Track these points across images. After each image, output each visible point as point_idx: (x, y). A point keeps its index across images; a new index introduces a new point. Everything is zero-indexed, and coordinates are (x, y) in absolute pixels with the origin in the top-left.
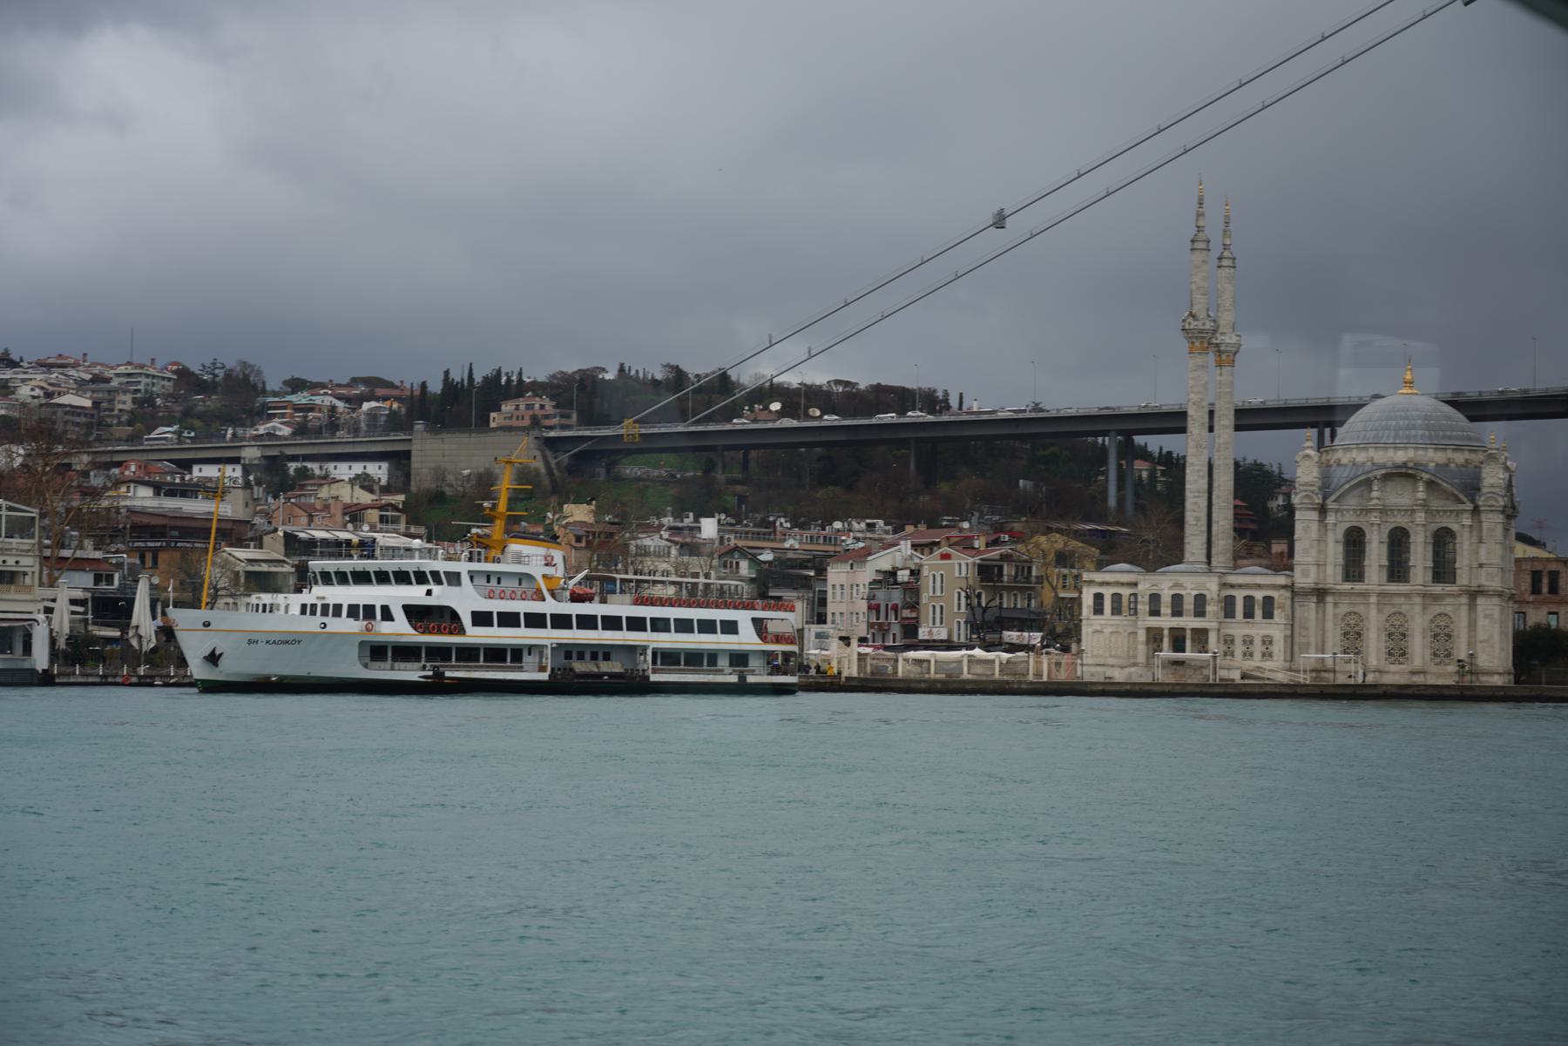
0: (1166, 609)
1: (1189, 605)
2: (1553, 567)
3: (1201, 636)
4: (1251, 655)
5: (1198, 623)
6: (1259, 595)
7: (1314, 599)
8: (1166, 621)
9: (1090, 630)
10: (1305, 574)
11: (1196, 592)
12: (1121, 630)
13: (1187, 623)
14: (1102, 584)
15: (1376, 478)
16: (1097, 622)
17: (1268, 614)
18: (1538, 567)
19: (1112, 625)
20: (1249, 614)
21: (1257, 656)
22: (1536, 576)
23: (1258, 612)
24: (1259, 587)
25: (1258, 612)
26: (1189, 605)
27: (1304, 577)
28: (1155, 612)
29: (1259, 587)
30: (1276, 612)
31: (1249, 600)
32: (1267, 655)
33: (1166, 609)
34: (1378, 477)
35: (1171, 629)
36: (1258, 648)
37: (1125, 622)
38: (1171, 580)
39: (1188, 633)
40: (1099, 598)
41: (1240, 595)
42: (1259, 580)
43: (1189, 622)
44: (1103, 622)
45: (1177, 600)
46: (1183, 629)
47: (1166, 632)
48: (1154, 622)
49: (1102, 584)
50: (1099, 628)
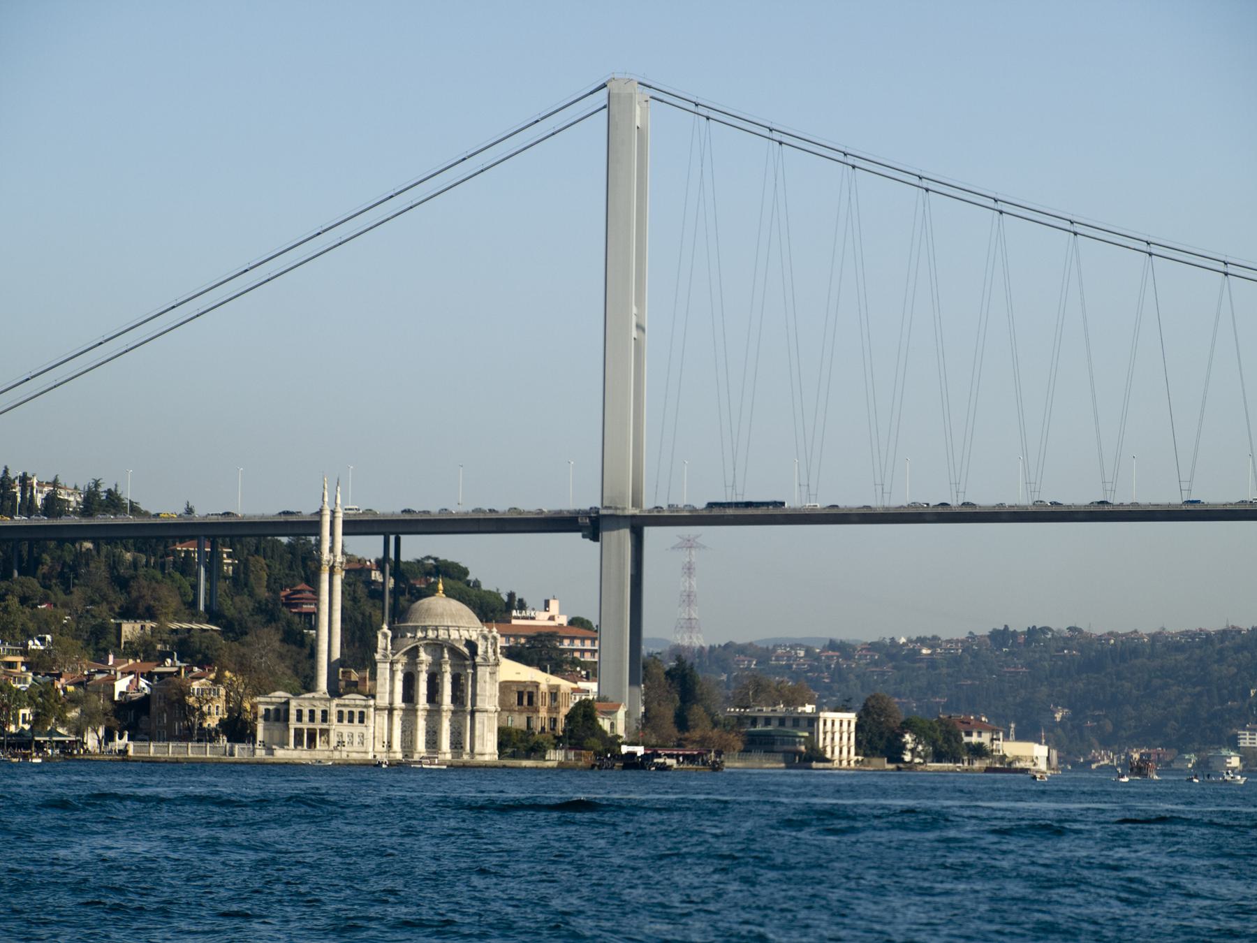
0: (306, 718)
1: (318, 715)
2: (530, 689)
3: (325, 732)
4: (352, 743)
5: (325, 726)
6: (356, 711)
7: (387, 712)
8: (306, 725)
10: (382, 698)
17: (361, 721)
18: (521, 689)
20: (351, 721)
21: (355, 743)
22: (520, 695)
23: (356, 720)
24: (356, 706)
25: (356, 720)
26: (318, 715)
27: (383, 700)
28: (299, 718)
29: (356, 706)
31: (351, 713)
33: (306, 718)
35: (308, 729)
36: (356, 739)
39: (318, 731)
40: (267, 711)
41: (346, 710)
42: (358, 702)
43: (318, 725)
45: (312, 712)
46: (315, 729)
47: (306, 731)
48: (299, 725)
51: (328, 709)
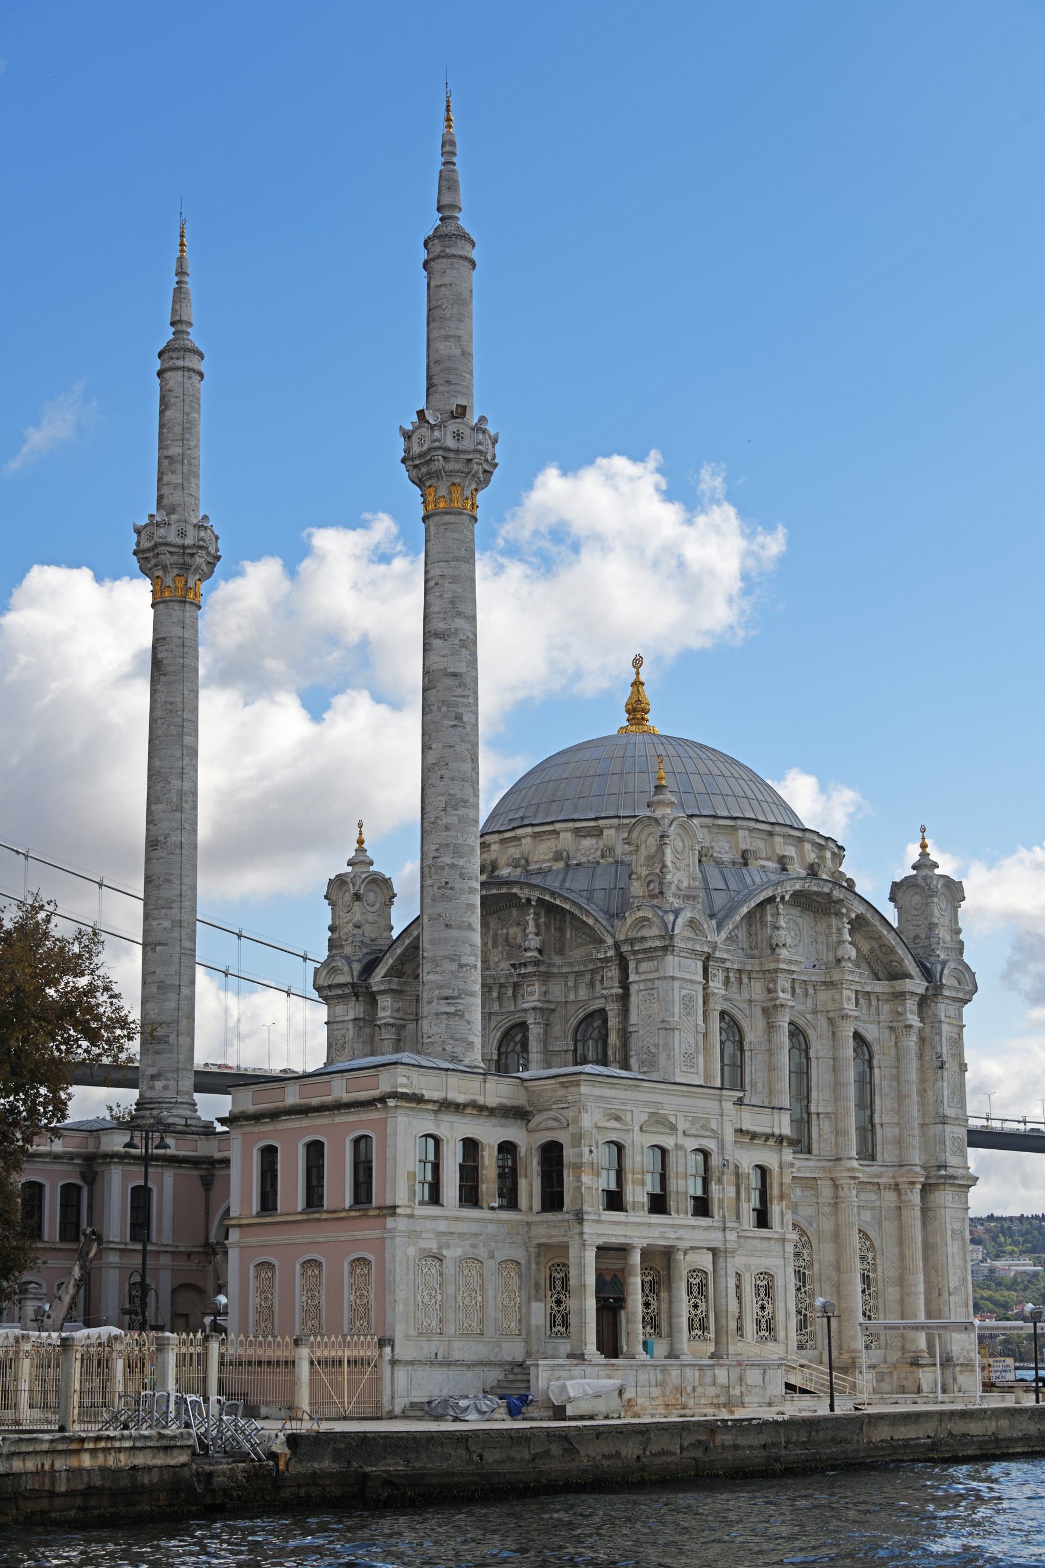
0: (637, 1194)
9: (411, 1251)
11: (691, 1144)
12: (482, 1252)
13: (681, 1233)
14: (446, 1106)
15: (783, 898)
16: (429, 1225)
19: (462, 1236)
30: (775, 1209)
32: (767, 1326)
34: (787, 898)
37: (491, 1228)
38: (647, 1103)
44: (442, 1226)
47: (636, 1258)
49: (446, 1106)
50: (433, 1245)
51: (711, 1145)
